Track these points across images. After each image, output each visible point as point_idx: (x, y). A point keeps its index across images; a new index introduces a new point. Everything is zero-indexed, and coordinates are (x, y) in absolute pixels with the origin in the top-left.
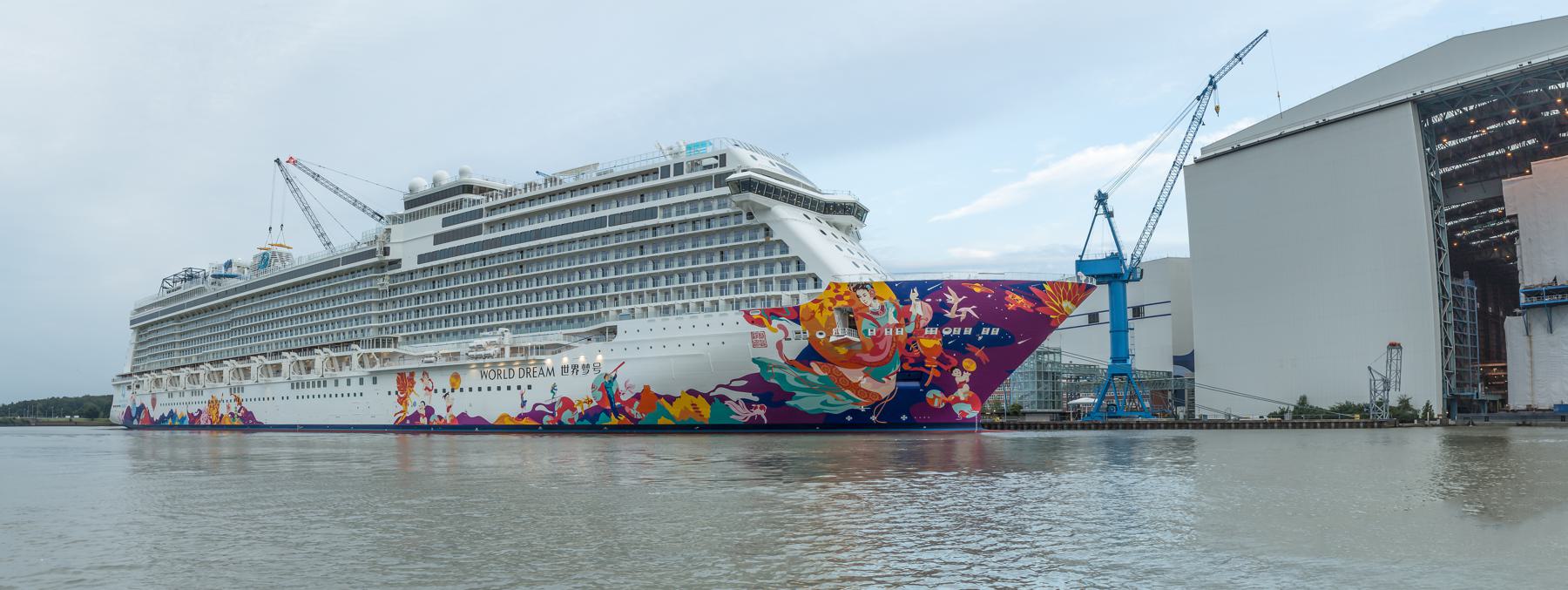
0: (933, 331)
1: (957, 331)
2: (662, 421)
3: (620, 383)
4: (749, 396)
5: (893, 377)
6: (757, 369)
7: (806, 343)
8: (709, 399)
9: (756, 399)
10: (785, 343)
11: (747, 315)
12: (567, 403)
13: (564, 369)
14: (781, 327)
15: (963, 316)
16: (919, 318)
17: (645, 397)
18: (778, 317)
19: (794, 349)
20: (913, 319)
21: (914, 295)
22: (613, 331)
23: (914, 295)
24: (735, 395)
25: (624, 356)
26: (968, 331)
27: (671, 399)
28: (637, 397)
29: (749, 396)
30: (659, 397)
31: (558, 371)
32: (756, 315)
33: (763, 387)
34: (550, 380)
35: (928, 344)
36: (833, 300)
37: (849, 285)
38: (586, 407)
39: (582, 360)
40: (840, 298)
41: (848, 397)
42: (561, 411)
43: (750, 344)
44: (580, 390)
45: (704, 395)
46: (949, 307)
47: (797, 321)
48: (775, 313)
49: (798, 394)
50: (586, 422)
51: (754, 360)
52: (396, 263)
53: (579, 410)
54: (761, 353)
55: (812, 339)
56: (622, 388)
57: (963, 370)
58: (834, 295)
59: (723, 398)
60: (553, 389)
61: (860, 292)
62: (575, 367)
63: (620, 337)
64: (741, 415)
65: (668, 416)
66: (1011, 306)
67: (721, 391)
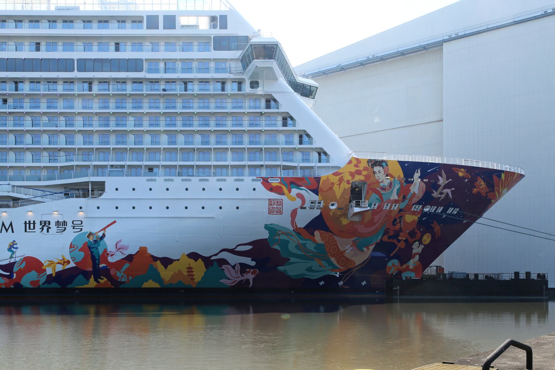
3: (109, 243)
4: (248, 261)
6: (265, 235)
7: (317, 213)
8: (207, 261)
9: (253, 263)
10: (299, 211)
11: (265, 182)
12: (33, 264)
13: (29, 225)
14: (300, 196)
16: (414, 194)
17: (141, 260)
18: (298, 186)
19: (304, 218)
21: (417, 175)
22: (100, 187)
23: (417, 175)
24: (233, 259)
25: (116, 214)
27: (166, 262)
28: (130, 258)
29: (248, 261)
30: (155, 259)
31: (19, 226)
32: (275, 183)
33: (264, 253)
34: (7, 238)
36: (352, 174)
37: (369, 161)
38: (59, 268)
39: (55, 217)
40: (359, 172)
41: (330, 263)
42: (21, 273)
43: (266, 210)
44: (53, 250)
48: (294, 183)
49: (292, 260)
50: (55, 285)
53: (49, 271)
54: (275, 220)
55: (326, 209)
56: (111, 248)
57: (421, 243)
58: (353, 169)
60: (12, 247)
61: (377, 169)
62: (45, 225)
63: (109, 192)
65: (157, 278)
67: (221, 256)
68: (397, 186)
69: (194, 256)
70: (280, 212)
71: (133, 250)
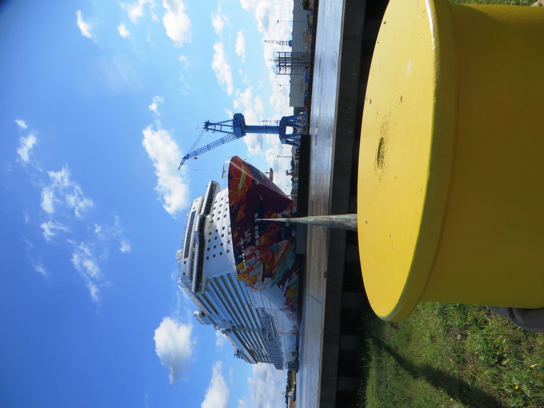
0: (257, 243)
1: (257, 232)
2: (297, 295)
5: (279, 244)
6: (276, 285)
9: (288, 279)
15: (249, 235)
20: (252, 252)
24: (287, 284)
26: (257, 228)
27: (288, 298)
35: (263, 239)
46: (245, 242)
47: (254, 283)
49: (286, 269)
50: (297, 310)
51: (272, 287)
52: (234, 327)
58: (243, 278)
59: (288, 286)
61: (241, 272)
64: (295, 277)
66: (243, 216)
67: (285, 289)
68: (248, 261)
69: (285, 296)
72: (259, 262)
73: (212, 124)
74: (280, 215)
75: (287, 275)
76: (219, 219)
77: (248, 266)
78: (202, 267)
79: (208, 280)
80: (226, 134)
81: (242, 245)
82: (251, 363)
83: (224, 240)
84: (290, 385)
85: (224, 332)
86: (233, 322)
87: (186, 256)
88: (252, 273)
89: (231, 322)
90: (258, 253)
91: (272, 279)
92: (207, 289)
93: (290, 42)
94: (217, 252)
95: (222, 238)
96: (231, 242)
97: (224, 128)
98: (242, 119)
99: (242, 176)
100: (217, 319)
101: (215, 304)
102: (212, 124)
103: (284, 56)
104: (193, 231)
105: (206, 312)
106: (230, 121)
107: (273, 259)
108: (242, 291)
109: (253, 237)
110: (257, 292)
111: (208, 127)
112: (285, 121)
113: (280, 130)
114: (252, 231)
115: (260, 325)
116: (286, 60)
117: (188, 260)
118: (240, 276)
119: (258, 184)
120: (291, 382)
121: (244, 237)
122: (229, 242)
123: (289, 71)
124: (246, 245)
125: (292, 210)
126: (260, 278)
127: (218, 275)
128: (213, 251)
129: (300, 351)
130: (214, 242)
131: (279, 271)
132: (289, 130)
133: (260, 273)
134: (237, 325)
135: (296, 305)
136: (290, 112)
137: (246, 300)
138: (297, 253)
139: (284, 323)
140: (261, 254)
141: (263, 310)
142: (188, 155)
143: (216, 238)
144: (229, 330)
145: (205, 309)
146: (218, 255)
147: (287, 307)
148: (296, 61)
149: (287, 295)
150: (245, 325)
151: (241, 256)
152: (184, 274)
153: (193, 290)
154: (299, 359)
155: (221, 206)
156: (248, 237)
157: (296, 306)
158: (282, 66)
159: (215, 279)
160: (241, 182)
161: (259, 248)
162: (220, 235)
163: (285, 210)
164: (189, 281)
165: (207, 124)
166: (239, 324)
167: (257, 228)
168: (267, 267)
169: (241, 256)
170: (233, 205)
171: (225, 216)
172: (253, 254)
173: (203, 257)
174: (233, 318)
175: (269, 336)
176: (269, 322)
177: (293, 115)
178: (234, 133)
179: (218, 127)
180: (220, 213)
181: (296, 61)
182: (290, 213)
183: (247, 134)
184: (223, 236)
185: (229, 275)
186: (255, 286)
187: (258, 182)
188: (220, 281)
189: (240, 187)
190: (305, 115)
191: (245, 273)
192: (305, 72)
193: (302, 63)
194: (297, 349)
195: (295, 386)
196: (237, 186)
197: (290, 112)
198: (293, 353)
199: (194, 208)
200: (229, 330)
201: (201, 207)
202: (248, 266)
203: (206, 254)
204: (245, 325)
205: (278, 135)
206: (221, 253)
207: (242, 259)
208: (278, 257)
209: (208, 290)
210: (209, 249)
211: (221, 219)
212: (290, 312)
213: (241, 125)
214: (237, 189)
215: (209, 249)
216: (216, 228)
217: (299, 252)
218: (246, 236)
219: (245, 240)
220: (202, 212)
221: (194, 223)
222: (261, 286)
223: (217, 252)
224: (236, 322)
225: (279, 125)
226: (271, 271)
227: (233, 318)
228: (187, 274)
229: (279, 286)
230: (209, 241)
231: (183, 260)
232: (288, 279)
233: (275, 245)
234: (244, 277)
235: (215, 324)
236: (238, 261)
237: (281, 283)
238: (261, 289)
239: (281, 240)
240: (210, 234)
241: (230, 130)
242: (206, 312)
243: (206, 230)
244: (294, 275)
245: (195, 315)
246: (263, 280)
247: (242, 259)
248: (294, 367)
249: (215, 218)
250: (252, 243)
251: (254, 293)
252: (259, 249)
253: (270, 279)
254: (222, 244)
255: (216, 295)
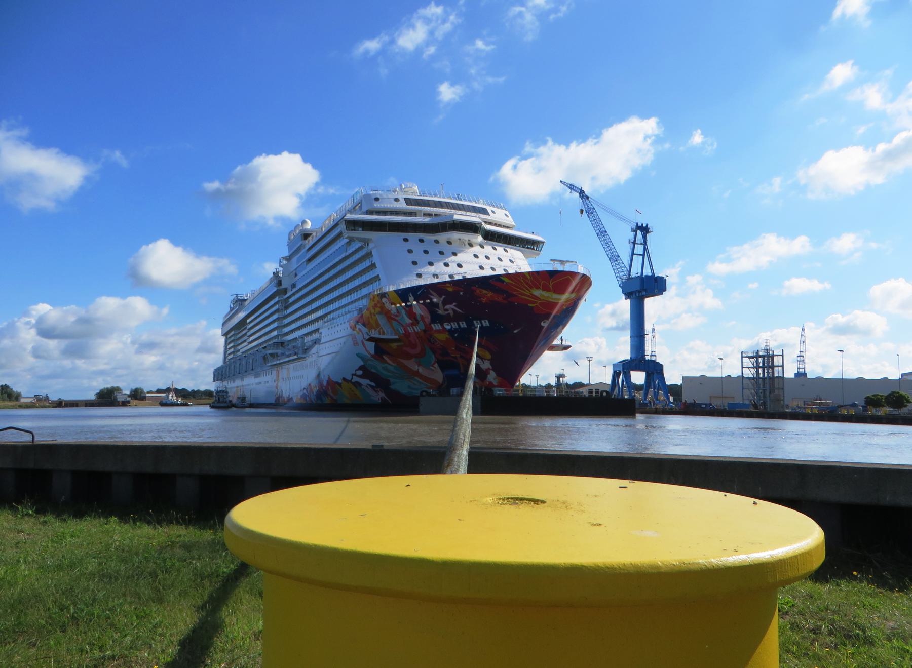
0: (436, 327)
1: (455, 325)
2: (346, 401)
5: (436, 365)
6: (362, 363)
9: (373, 384)
15: (451, 312)
16: (422, 316)
19: (371, 346)
20: (419, 318)
24: (365, 382)
26: (463, 325)
35: (443, 337)
37: (378, 295)
45: (351, 381)
46: (436, 305)
47: (364, 325)
49: (392, 380)
50: (319, 402)
52: (285, 291)
61: (384, 300)
64: (378, 396)
67: (355, 379)
68: (403, 312)
69: (344, 379)
70: (357, 344)
71: (327, 378)
72: (402, 331)
73: (645, 237)
74: (486, 365)
75: (381, 383)
76: (476, 256)
77: (394, 311)
78: (390, 231)
79: (366, 242)
80: (627, 263)
81: (431, 300)
82: (224, 324)
83: (438, 268)
84: (187, 396)
85: (276, 274)
86: (294, 290)
87: (409, 201)
88: (382, 320)
89: (294, 286)
90: (419, 328)
91: (372, 356)
92: (351, 240)
93: (804, 374)
94: (418, 255)
95: (442, 264)
96: (436, 281)
97: (637, 260)
98: (656, 291)
99: (555, 296)
100: (298, 261)
101: (326, 256)
102: (645, 237)
103: (776, 363)
104: (453, 211)
105: (310, 241)
106: (652, 270)
107: (409, 356)
108: (349, 304)
109: (448, 319)
110: (350, 331)
111: (639, 232)
112: (654, 370)
113: (639, 360)
114: (456, 318)
115: (289, 337)
116: (770, 367)
117: (402, 205)
118: (377, 299)
119: (542, 324)
120: (194, 397)
121: (445, 303)
122: (436, 276)
123: (749, 373)
124: (432, 307)
125: (497, 386)
126: (375, 334)
127: (376, 259)
128: (418, 248)
129: (248, 410)
130: (434, 250)
131: (386, 368)
132: (638, 378)
133: (384, 333)
134: (289, 297)
135: (327, 401)
136: (672, 377)
137: (334, 311)
138: (421, 399)
139: (296, 379)
140: (417, 333)
141: (316, 342)
142: (587, 198)
143: (441, 253)
144: (279, 283)
145: (315, 240)
146: (412, 257)
147: (325, 383)
148: (767, 386)
149: (344, 384)
150: (289, 311)
151: (411, 298)
152: (377, 199)
153: (349, 216)
154: (234, 409)
155: (500, 259)
156: (447, 310)
157: (326, 400)
158: (757, 362)
159: (369, 255)
160: (546, 294)
161: (427, 330)
162: (447, 261)
163: (498, 374)
164: (365, 209)
165: (645, 230)
166: (291, 300)
167: (463, 325)
168: (394, 345)
169: (411, 298)
170: (503, 281)
171: (481, 268)
172: (416, 319)
173: (406, 231)
174: (301, 289)
175: (272, 355)
176: (296, 354)
177: (668, 383)
178: (629, 278)
179: (639, 249)
180: (487, 258)
181: (767, 386)
182: (491, 383)
183: (629, 301)
184: (446, 265)
185: (377, 278)
186: (359, 326)
187: (545, 324)
188: (366, 264)
189: (537, 292)
190: (667, 405)
191: (382, 307)
192: (746, 402)
193: (764, 397)
194: (252, 406)
195: (186, 405)
196: (537, 288)
197: (672, 377)
198: (243, 399)
199: (493, 212)
200: (279, 283)
201: (496, 225)
202: (394, 311)
203: (413, 237)
204: (289, 311)
205: (628, 357)
206: (415, 263)
207: (406, 300)
208: (412, 364)
209: (348, 244)
210: (421, 241)
211: (477, 261)
212: (315, 390)
213: (645, 290)
214: (531, 288)
215: (421, 241)
216: (460, 251)
217: (423, 401)
218: (447, 307)
219: (441, 305)
220: (488, 227)
221: (468, 213)
222: (359, 338)
223: (418, 255)
224: (294, 294)
225: (647, 358)
226: (387, 353)
227: (301, 289)
228: (377, 205)
229: (361, 368)
230: (437, 242)
231: (401, 197)
232: (373, 384)
233: (433, 359)
234: (376, 306)
235: (289, 259)
236: (403, 294)
237: (366, 372)
238: (354, 337)
239: (443, 369)
240: (449, 243)
241: (636, 271)
242: (310, 241)
243: (455, 236)
244: (382, 395)
245: (304, 222)
246: (371, 339)
247: (406, 300)
248: (220, 401)
249: (476, 249)
250: (436, 318)
251: (347, 325)
252: (425, 331)
253: (373, 352)
254: (431, 264)
255: (340, 258)
